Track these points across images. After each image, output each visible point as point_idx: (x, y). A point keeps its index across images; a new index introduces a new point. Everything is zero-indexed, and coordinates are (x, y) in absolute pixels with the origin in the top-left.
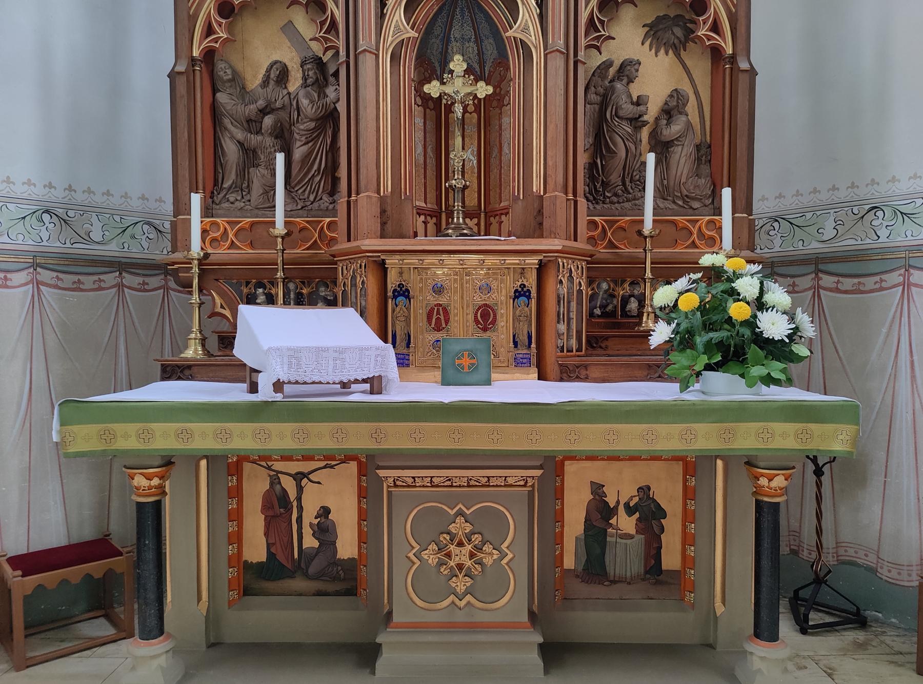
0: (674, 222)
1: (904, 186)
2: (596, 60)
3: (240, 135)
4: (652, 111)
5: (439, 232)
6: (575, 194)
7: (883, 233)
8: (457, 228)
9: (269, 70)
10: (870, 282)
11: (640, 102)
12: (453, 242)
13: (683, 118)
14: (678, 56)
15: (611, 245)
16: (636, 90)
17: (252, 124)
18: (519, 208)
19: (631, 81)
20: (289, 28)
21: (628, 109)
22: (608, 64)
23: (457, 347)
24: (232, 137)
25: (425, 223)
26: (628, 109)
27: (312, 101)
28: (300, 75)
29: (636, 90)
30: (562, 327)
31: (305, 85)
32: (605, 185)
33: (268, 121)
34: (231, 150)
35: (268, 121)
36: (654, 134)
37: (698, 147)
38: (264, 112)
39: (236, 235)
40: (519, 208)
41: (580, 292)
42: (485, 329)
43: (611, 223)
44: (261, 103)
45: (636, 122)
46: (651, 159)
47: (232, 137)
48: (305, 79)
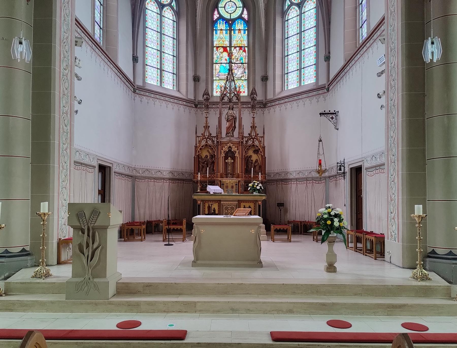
0: (256, 176)
1: (291, 170)
2: (246, 155)
3: (202, 164)
4: (254, 161)
5: (227, 177)
6: (243, 173)
7: (289, 176)
8: (229, 177)
9: (205, 157)
10: (270, 184)
11: (252, 161)
12: (228, 178)
13: (257, 163)
14: (257, 155)
15: (248, 178)
16: (252, 159)
17: (204, 163)
18: (236, 175)
19: (251, 158)
20: (208, 151)
21: (251, 161)
22: (248, 156)
23: (229, 190)
24: (201, 165)
25: (225, 176)
26: (251, 161)
27: (211, 160)
28: (209, 156)
29: (252, 159)
30: (241, 188)
31: (210, 158)
32: (248, 171)
33: (206, 163)
34: (201, 166)
35: (206, 163)
36: (254, 165)
37: (260, 166)
38: (205, 161)
39: (201, 177)
40: (236, 175)
41: (243, 184)
42: (232, 188)
43: (248, 176)
44: (205, 160)
45: (252, 163)
46: (252, 168)
47: (201, 165)
48: (210, 157)
